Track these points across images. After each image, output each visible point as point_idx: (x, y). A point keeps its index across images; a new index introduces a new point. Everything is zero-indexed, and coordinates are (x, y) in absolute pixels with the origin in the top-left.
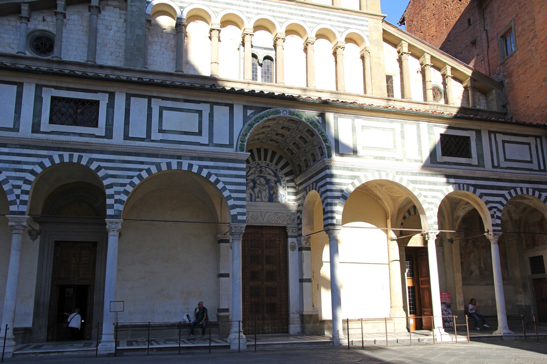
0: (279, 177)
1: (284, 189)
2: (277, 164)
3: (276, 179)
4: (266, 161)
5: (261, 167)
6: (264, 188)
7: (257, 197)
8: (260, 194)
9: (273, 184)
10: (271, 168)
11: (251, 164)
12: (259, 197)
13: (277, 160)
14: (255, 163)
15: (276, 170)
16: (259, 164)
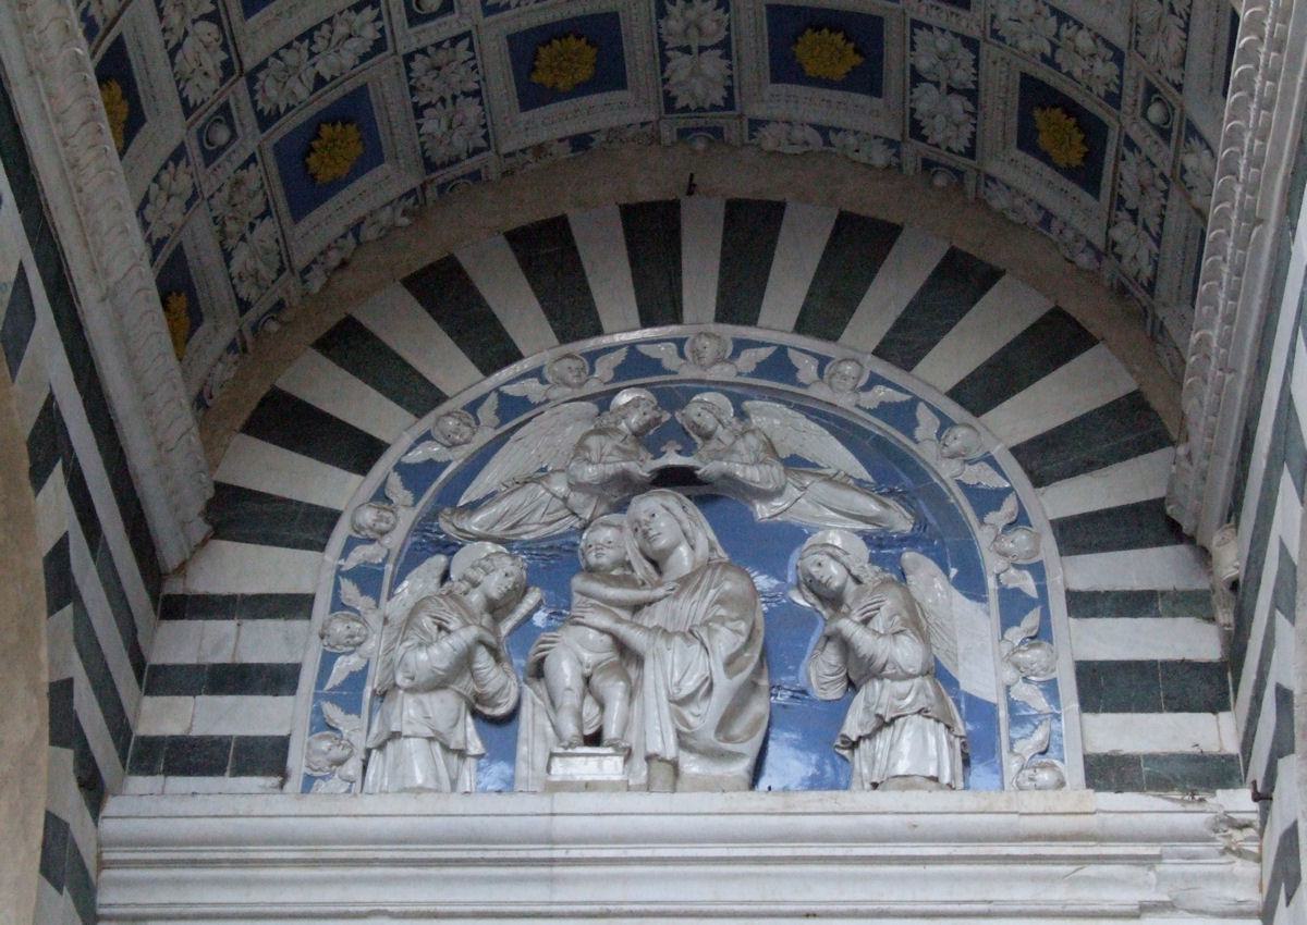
0: (937, 496)
1: (1016, 634)
2: (905, 346)
3: (901, 522)
4: (751, 320)
5: (672, 397)
6: (692, 607)
7: (570, 729)
8: (615, 691)
9: (833, 573)
10: (821, 392)
11: (537, 373)
12: (611, 732)
13: (912, 307)
14: (592, 357)
15: (902, 415)
16: (656, 366)
